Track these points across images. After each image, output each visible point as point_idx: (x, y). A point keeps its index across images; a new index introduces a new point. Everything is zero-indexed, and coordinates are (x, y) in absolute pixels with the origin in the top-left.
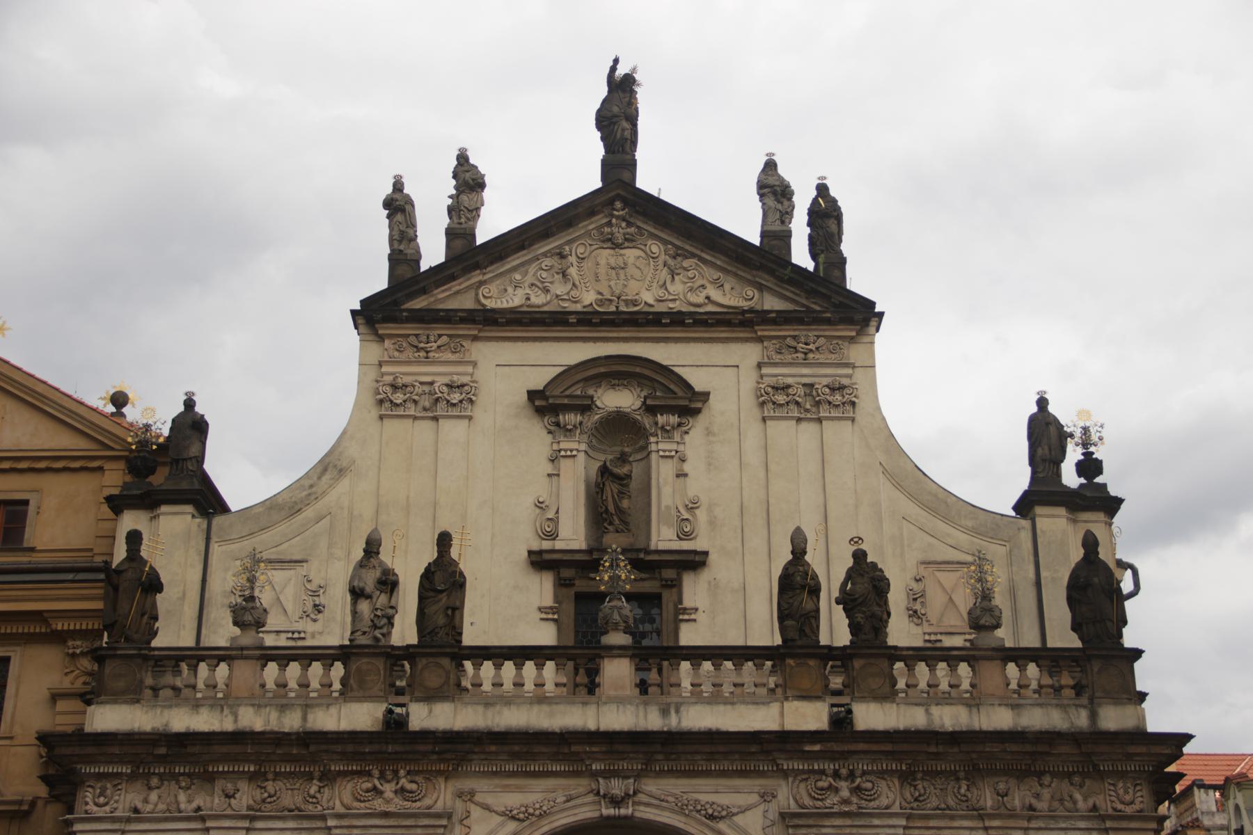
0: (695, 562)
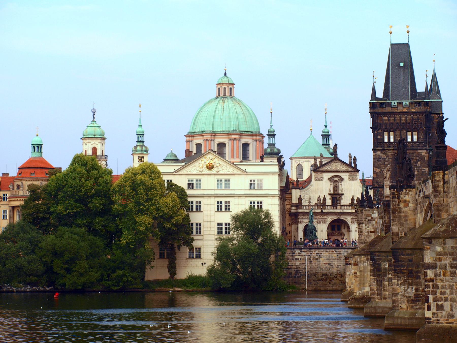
0: (343, 194)
